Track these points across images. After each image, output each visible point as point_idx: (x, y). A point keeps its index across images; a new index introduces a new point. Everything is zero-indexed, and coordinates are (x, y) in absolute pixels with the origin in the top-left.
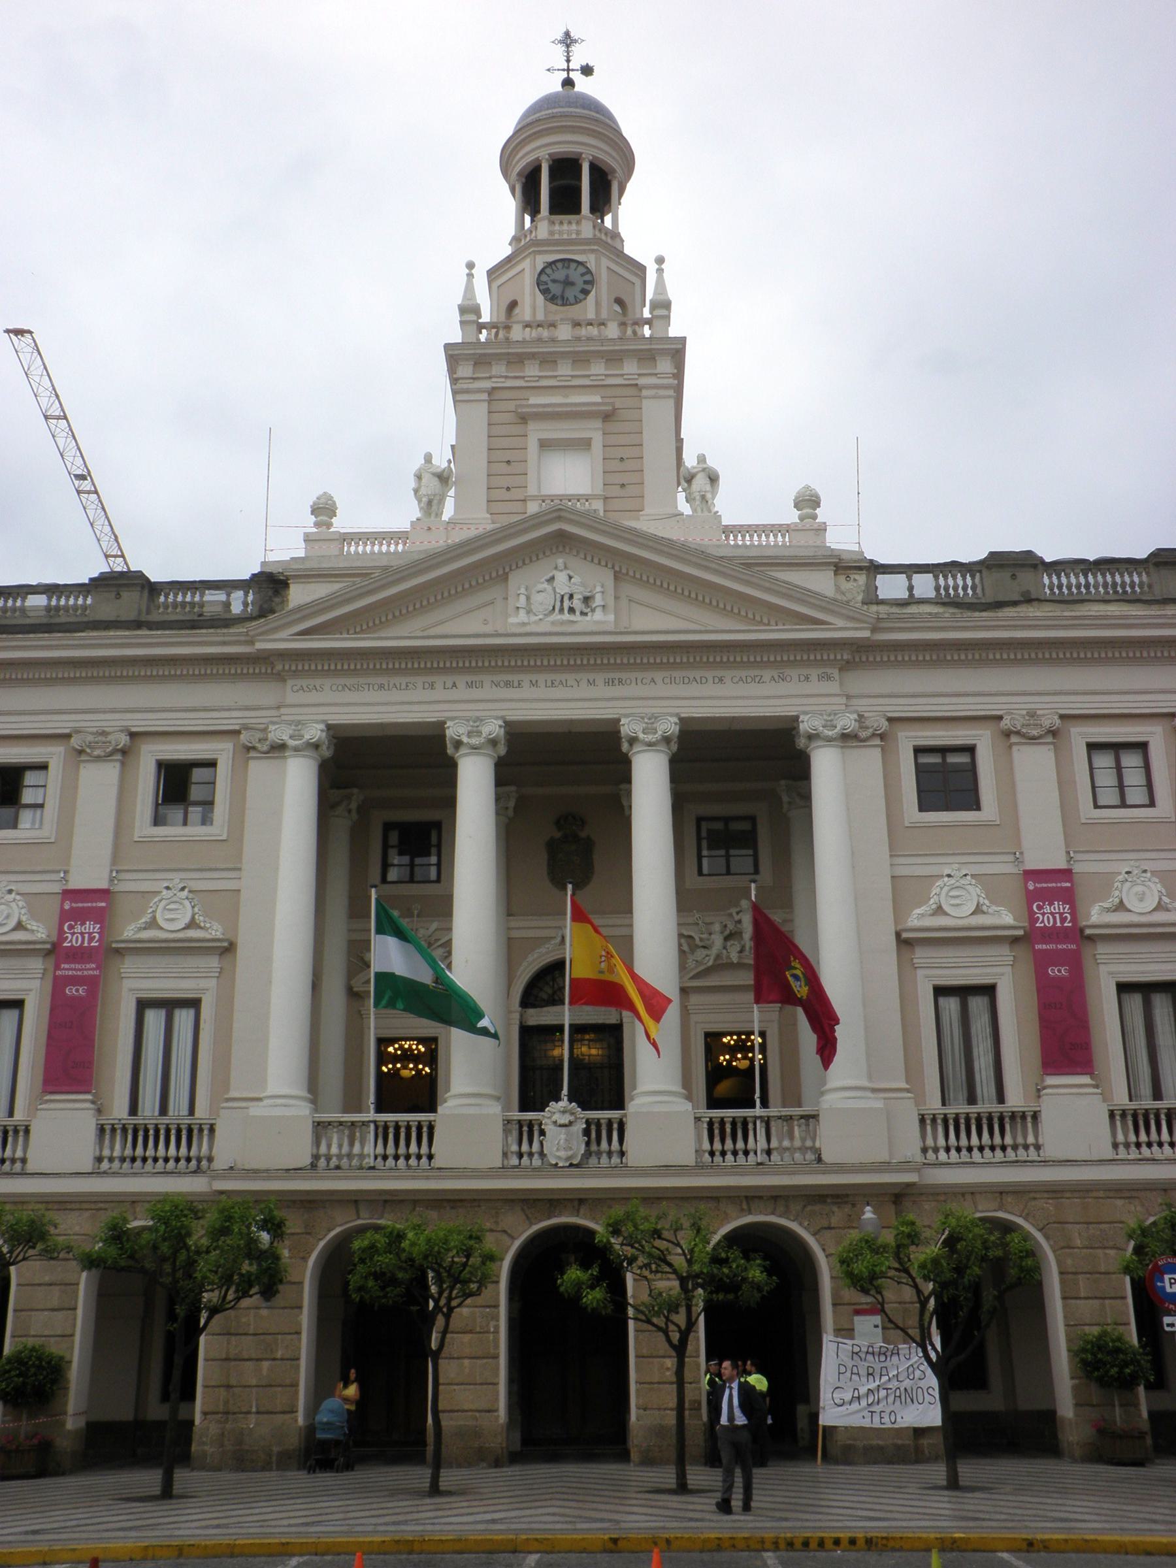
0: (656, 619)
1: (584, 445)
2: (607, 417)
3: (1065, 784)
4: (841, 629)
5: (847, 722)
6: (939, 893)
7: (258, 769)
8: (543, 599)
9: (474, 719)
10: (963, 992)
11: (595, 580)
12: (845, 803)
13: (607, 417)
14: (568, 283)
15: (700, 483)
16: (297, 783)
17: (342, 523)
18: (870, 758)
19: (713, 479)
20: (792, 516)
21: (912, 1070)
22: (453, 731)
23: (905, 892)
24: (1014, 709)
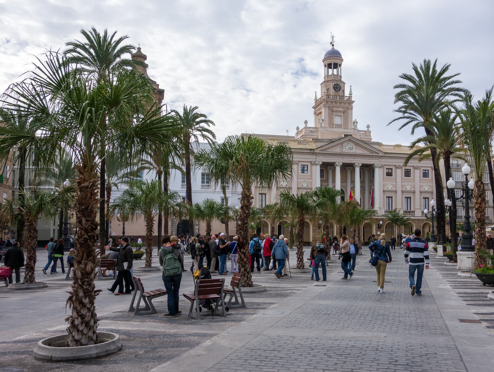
0: (359, 151)
1: (341, 116)
2: (344, 112)
3: (402, 174)
4: (381, 154)
5: (380, 165)
6: (388, 186)
7: (314, 167)
8: (348, 148)
9: (339, 161)
10: (389, 197)
11: (352, 145)
12: (379, 174)
13: (344, 112)
14: (337, 88)
15: (355, 124)
16: (318, 168)
17: (308, 125)
18: (381, 169)
19: (357, 123)
20: (366, 129)
21: (384, 206)
22: (337, 163)
23: (384, 185)
24: (397, 164)
